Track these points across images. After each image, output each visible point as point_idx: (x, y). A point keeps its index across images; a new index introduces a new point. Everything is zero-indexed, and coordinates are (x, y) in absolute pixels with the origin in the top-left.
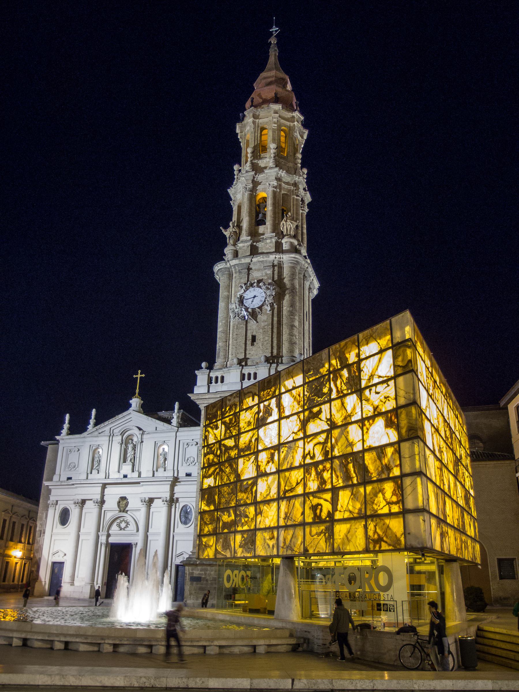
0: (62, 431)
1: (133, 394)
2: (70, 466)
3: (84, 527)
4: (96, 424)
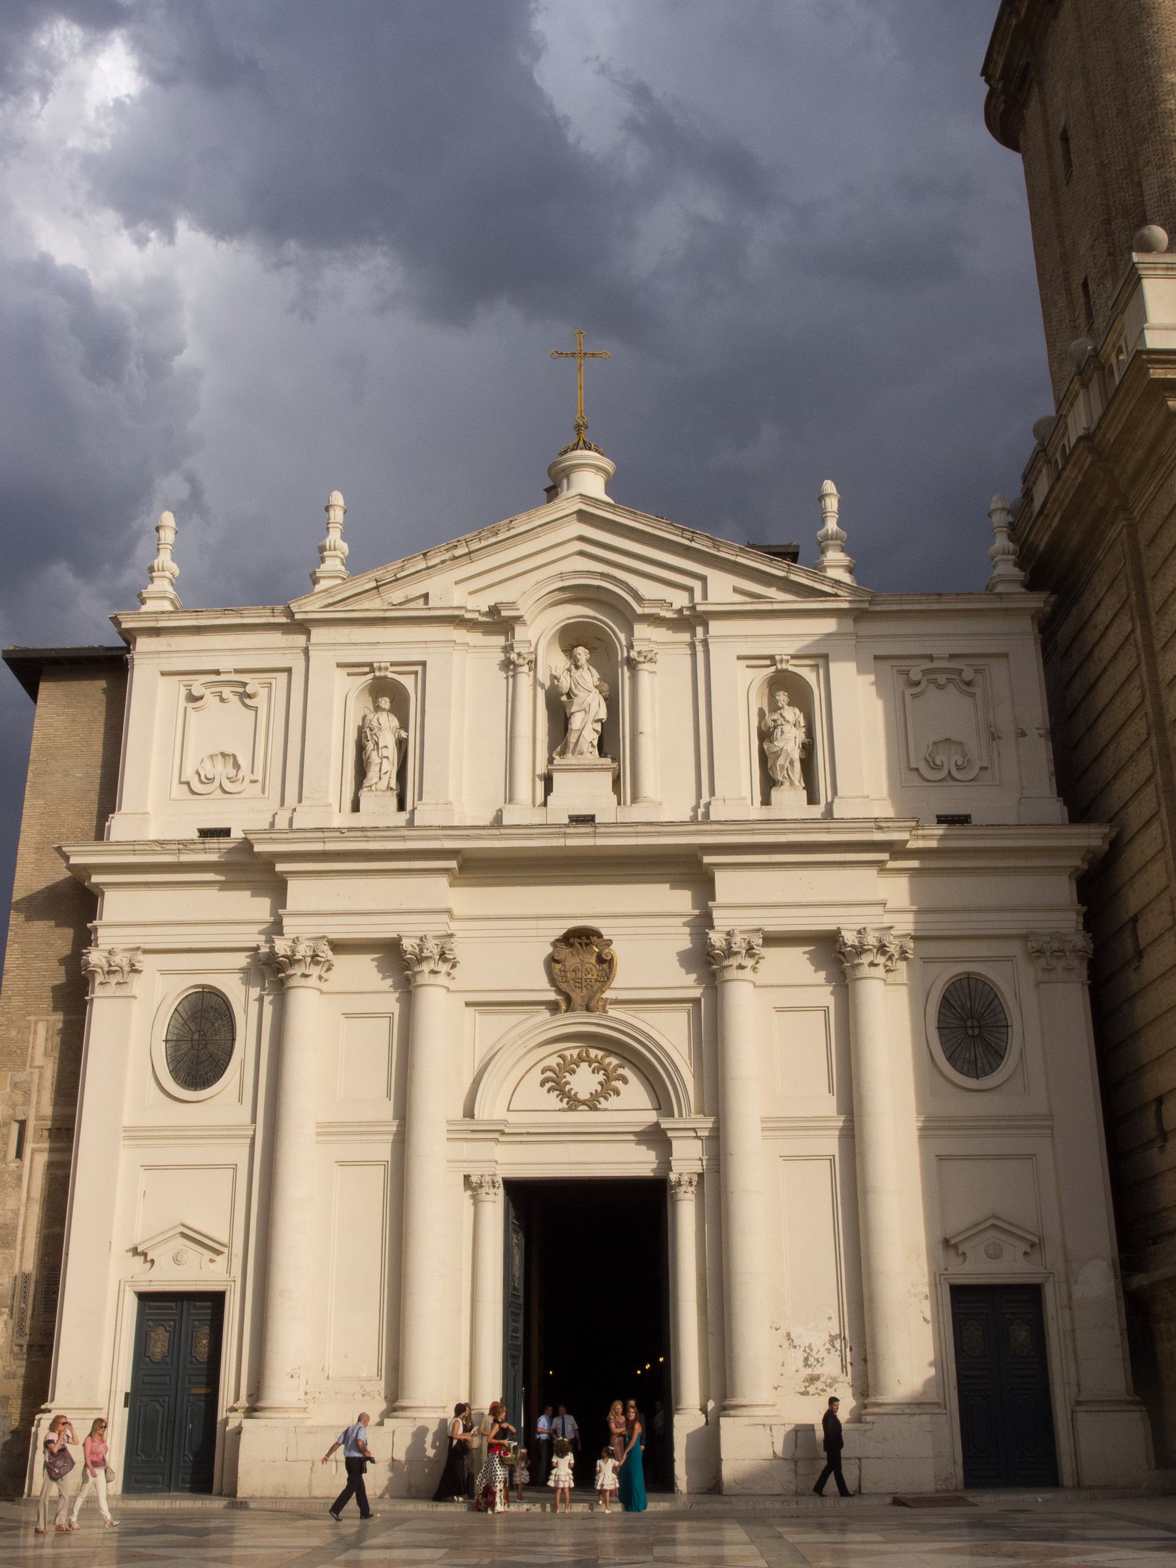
4: (355, 565)
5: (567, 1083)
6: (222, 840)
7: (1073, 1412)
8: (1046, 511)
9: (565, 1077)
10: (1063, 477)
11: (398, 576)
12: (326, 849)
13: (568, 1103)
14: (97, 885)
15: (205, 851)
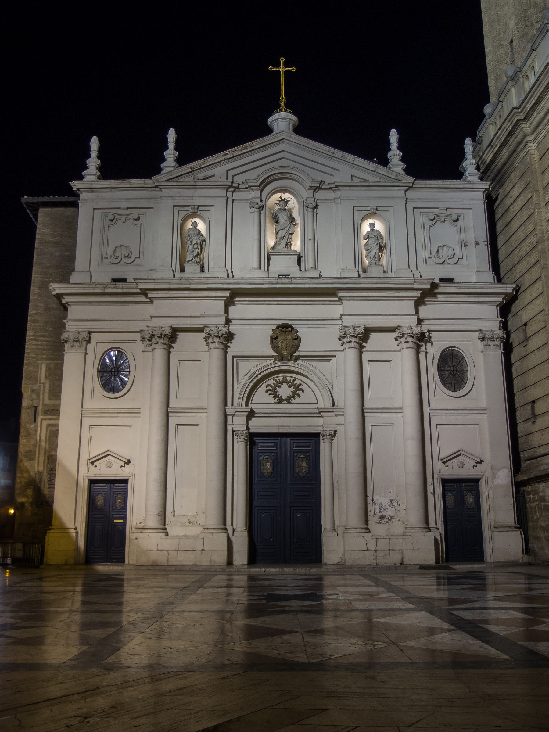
0: (83, 173)
1: (276, 107)
2: (117, 255)
3: (177, 396)
4: (181, 161)
5: (277, 392)
6: (124, 283)
7: (491, 531)
8: (492, 144)
9: (276, 389)
10: (503, 127)
11: (202, 166)
12: (171, 287)
13: (278, 400)
14: (67, 303)
15: (116, 288)
